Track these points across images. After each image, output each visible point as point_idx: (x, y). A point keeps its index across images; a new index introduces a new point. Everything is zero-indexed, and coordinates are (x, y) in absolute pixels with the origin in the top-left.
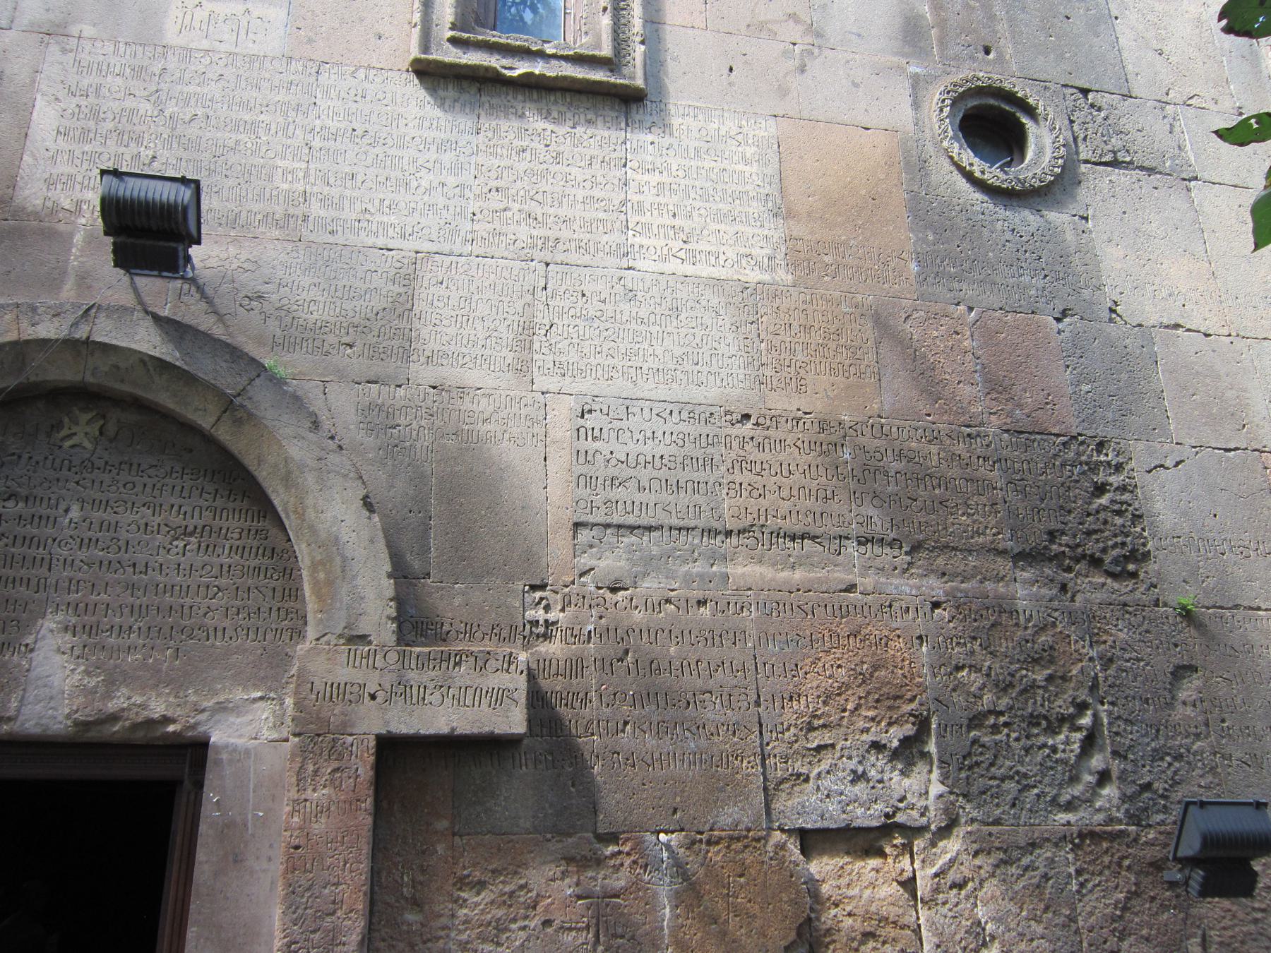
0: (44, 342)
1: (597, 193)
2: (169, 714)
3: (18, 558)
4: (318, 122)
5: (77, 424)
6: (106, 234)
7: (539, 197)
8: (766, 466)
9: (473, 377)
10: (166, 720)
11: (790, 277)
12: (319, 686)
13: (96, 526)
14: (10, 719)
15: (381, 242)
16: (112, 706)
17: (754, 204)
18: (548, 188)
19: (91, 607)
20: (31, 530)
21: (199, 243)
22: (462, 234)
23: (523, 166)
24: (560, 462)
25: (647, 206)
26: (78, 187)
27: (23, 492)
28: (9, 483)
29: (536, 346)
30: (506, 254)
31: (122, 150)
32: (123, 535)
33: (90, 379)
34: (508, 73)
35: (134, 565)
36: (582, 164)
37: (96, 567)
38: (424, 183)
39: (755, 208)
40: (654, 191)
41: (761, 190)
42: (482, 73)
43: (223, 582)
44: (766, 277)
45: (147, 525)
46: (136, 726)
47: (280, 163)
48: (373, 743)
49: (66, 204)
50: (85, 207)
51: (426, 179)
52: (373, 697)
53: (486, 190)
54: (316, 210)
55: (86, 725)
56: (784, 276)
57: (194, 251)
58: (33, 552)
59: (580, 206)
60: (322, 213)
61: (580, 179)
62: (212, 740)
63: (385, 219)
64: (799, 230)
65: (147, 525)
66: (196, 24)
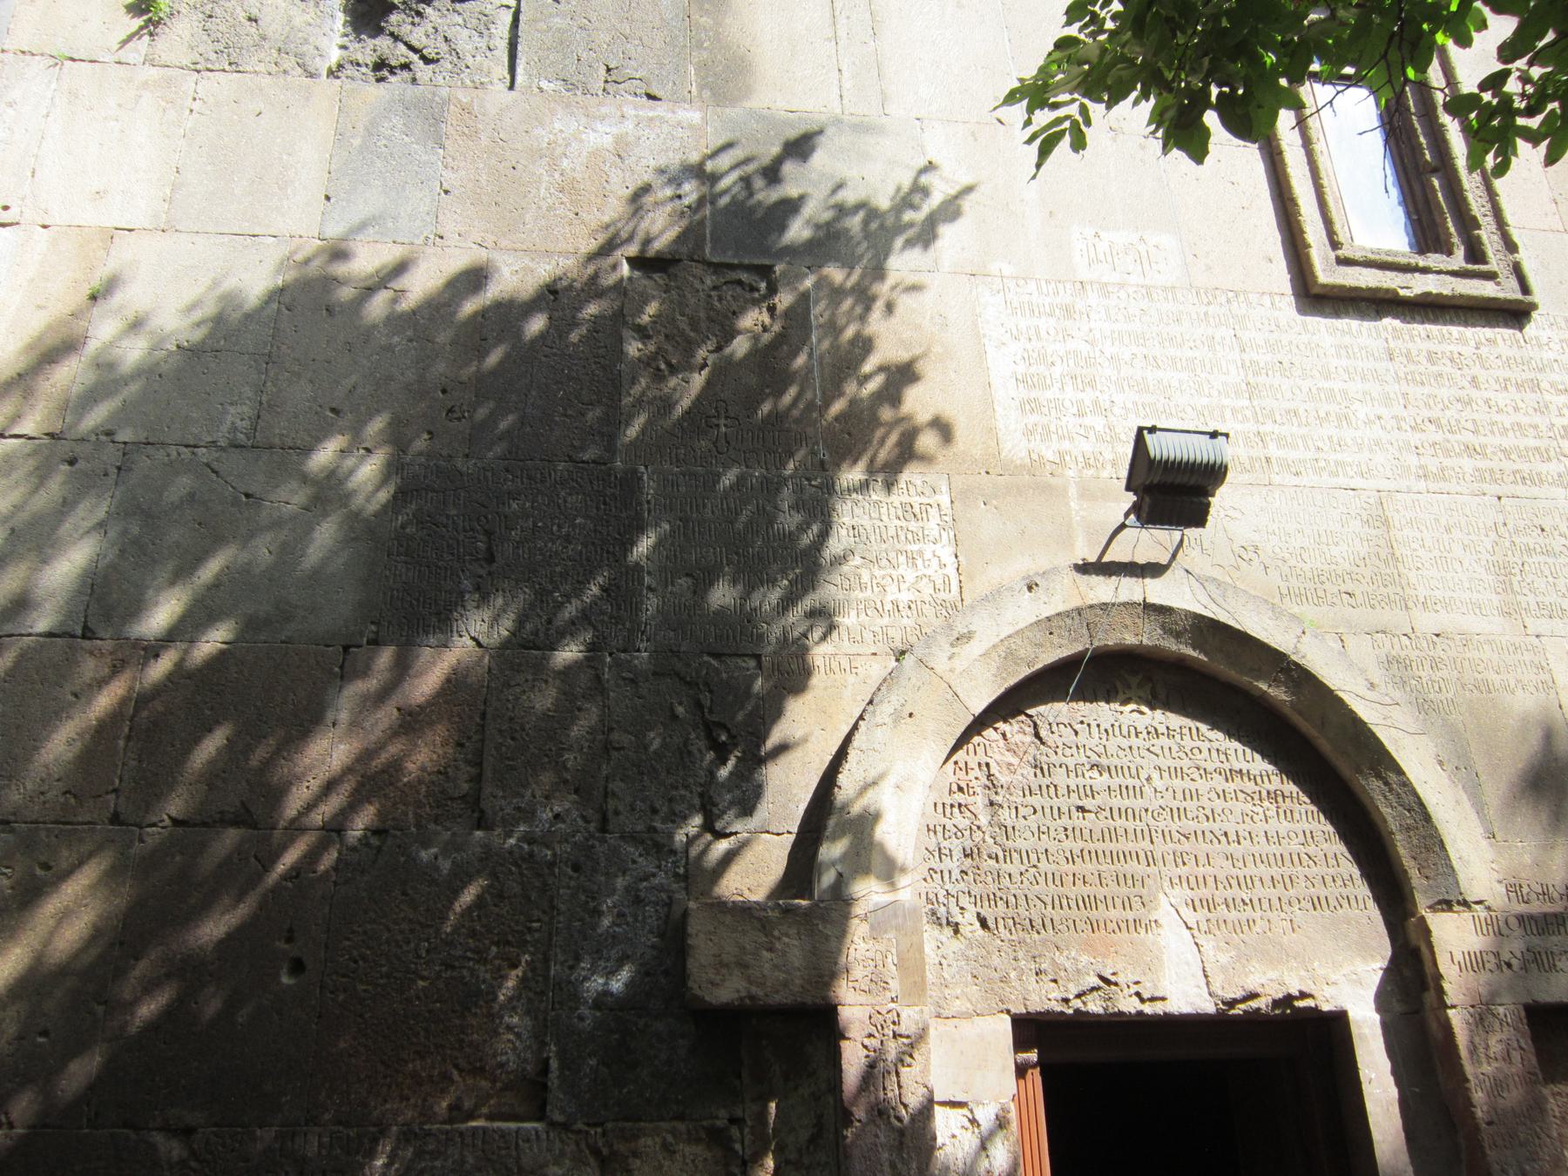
0: (1104, 607)
1: (1525, 420)
2: (1305, 989)
3: (1121, 832)
4: (1245, 356)
5: (1129, 687)
6: (1128, 488)
7: (1470, 425)
9: (1475, 624)
10: (1303, 995)
12: (1458, 957)
13: (1179, 795)
14: (1163, 999)
15: (1342, 481)
16: (1252, 984)
18: (1476, 416)
19: (1201, 880)
20: (1116, 802)
22: (1413, 470)
23: (1444, 393)
26: (1054, 437)
27: (1104, 761)
28: (1089, 753)
29: (1515, 584)
30: (1459, 489)
31: (1080, 396)
32: (1207, 804)
33: (1145, 642)
34: (1402, 293)
35: (1226, 834)
37: (1192, 837)
38: (1361, 416)
42: (1381, 295)
43: (1311, 849)
46: (1276, 1003)
47: (1226, 402)
48: (1523, 1014)
49: (1050, 455)
50: (1067, 458)
51: (1362, 411)
52: (1509, 965)
54: (1273, 451)
55: (1232, 1003)
58: (1130, 825)
59: (1511, 434)
60: (1281, 453)
61: (1502, 405)
62: (1351, 1014)
63: (1339, 456)
66: (1101, 257)
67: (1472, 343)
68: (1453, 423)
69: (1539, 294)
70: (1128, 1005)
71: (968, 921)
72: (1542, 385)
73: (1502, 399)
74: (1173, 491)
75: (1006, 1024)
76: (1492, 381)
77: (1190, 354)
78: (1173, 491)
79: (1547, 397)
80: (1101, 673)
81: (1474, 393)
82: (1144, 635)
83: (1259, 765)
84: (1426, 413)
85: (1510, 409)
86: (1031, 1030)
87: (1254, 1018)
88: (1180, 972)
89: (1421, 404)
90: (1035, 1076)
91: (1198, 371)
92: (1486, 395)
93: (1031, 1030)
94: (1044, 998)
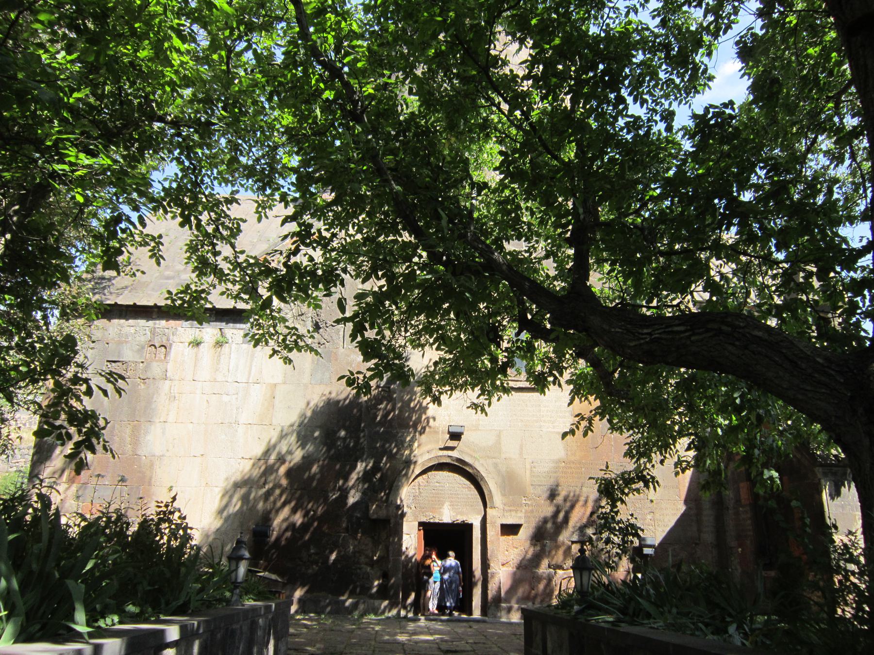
24: (528, 472)
54: (481, 422)
70: (437, 521)
71: (413, 508)
74: (456, 436)
75: (417, 523)
78: (456, 436)
80: (440, 467)
82: (448, 461)
83: (468, 483)
86: (421, 524)
87: (458, 524)
88: (447, 516)
90: (422, 531)
93: (421, 524)
94: (424, 519)
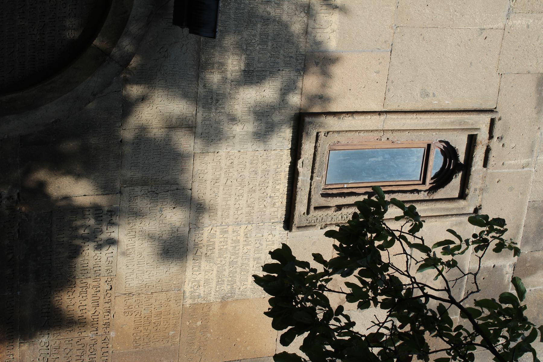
1: (231, 212)
4: (268, 72)
8: (85, 298)
11: (188, 306)
17: (229, 287)
18: (234, 187)
21: (190, 33)
23: (246, 173)
25: (225, 236)
36: (249, 202)
39: (226, 288)
40: (234, 238)
41: (237, 290)
44: (187, 294)
45: (44, 16)
53: (232, 157)
56: (188, 302)
57: (186, 30)
59: (224, 203)
61: (240, 202)
64: (215, 309)
65: (44, 16)
67: (273, 195)
68: (231, 174)
69: (295, 233)
72: (250, 226)
73: (243, 203)
76: (253, 200)
77: (270, 44)
79: (243, 227)
81: (246, 189)
84: (236, 162)
85: (237, 206)
89: (241, 160)
91: (261, 47)
92: (245, 195)
